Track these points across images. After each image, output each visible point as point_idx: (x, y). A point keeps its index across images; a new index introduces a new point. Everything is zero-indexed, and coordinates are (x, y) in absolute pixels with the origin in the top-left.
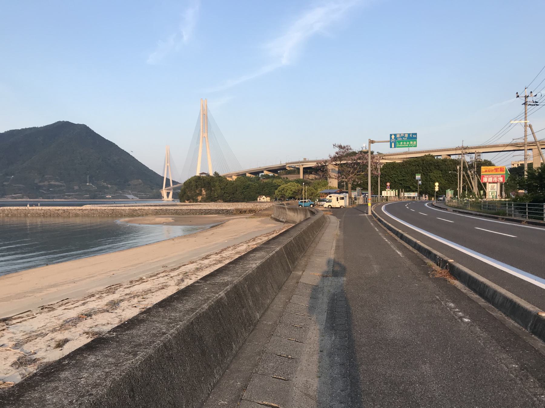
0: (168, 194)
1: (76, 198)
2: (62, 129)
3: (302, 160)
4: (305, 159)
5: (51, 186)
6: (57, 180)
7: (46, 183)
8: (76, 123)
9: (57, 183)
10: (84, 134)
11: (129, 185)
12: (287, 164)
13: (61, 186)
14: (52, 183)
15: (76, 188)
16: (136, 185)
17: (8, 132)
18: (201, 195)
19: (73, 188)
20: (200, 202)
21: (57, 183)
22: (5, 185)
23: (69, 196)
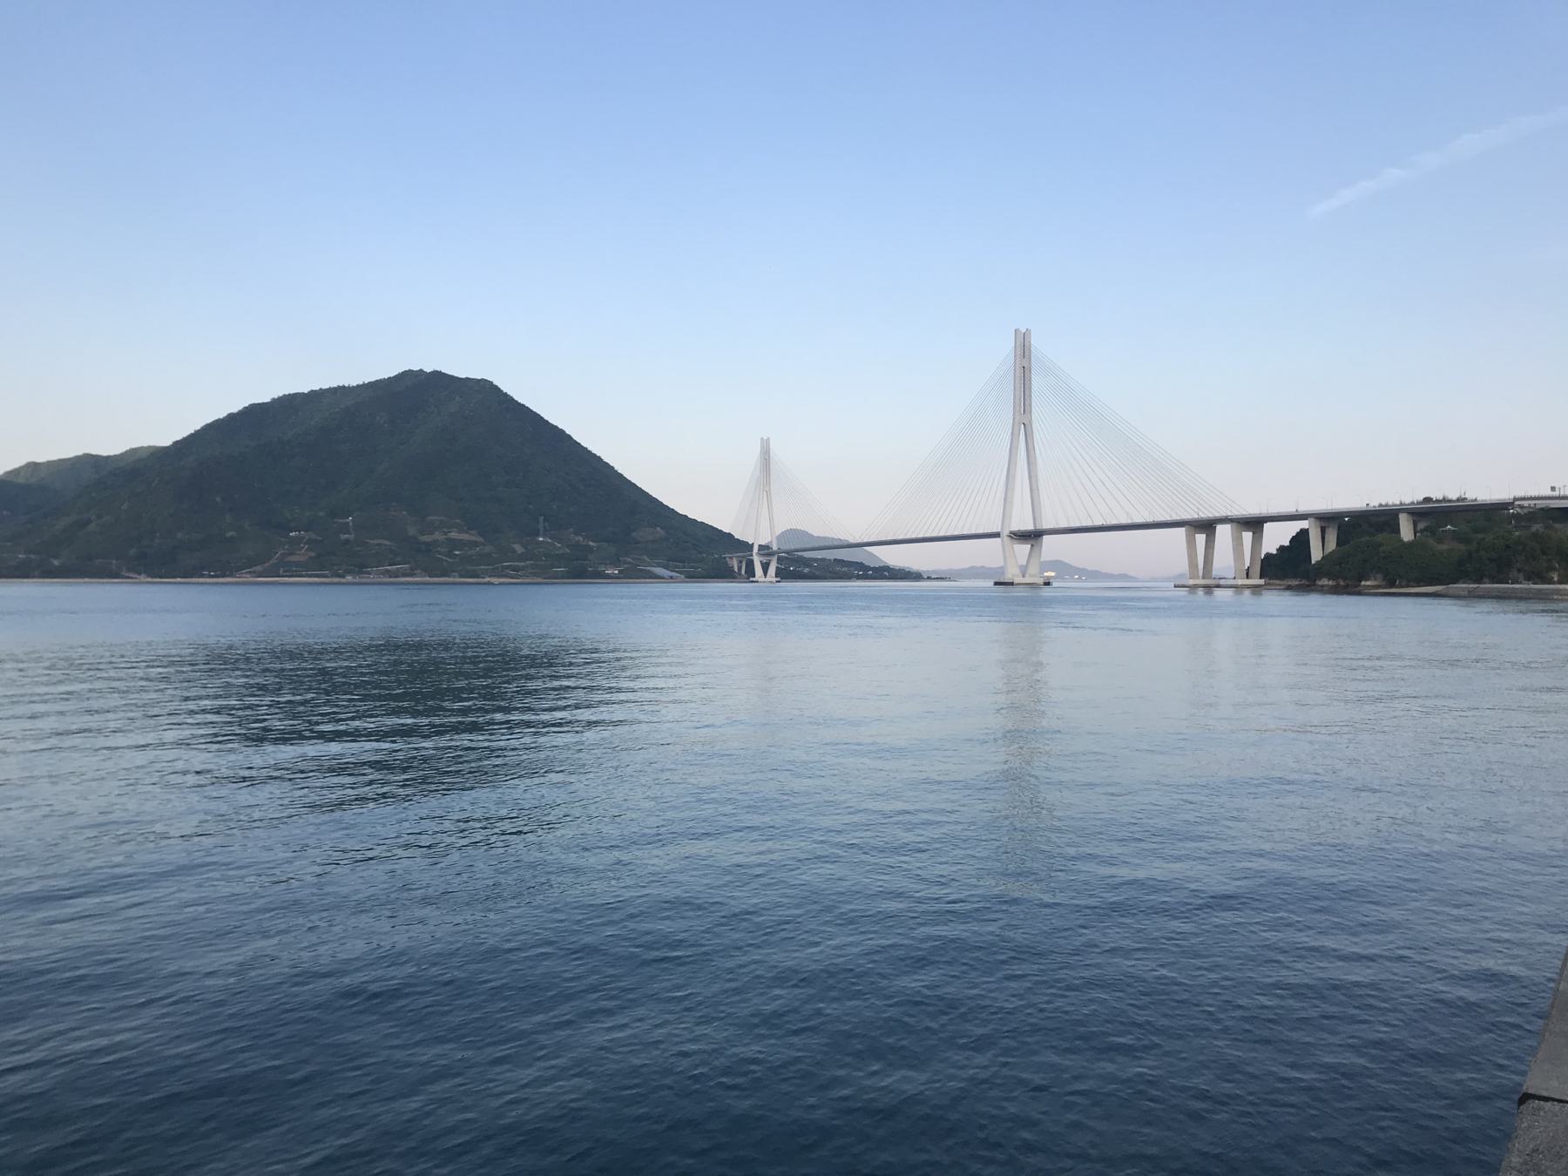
0: (765, 567)
1: (535, 575)
2: (419, 393)
3: (1549, 493)
4: (1553, 489)
7: (438, 536)
8: (463, 376)
9: (465, 537)
12: (1516, 499)
13: (476, 544)
14: (454, 535)
15: (519, 549)
18: (1554, 569)
19: (514, 551)
20: (1560, 582)
21: (465, 537)
22: (347, 541)
23: (516, 569)
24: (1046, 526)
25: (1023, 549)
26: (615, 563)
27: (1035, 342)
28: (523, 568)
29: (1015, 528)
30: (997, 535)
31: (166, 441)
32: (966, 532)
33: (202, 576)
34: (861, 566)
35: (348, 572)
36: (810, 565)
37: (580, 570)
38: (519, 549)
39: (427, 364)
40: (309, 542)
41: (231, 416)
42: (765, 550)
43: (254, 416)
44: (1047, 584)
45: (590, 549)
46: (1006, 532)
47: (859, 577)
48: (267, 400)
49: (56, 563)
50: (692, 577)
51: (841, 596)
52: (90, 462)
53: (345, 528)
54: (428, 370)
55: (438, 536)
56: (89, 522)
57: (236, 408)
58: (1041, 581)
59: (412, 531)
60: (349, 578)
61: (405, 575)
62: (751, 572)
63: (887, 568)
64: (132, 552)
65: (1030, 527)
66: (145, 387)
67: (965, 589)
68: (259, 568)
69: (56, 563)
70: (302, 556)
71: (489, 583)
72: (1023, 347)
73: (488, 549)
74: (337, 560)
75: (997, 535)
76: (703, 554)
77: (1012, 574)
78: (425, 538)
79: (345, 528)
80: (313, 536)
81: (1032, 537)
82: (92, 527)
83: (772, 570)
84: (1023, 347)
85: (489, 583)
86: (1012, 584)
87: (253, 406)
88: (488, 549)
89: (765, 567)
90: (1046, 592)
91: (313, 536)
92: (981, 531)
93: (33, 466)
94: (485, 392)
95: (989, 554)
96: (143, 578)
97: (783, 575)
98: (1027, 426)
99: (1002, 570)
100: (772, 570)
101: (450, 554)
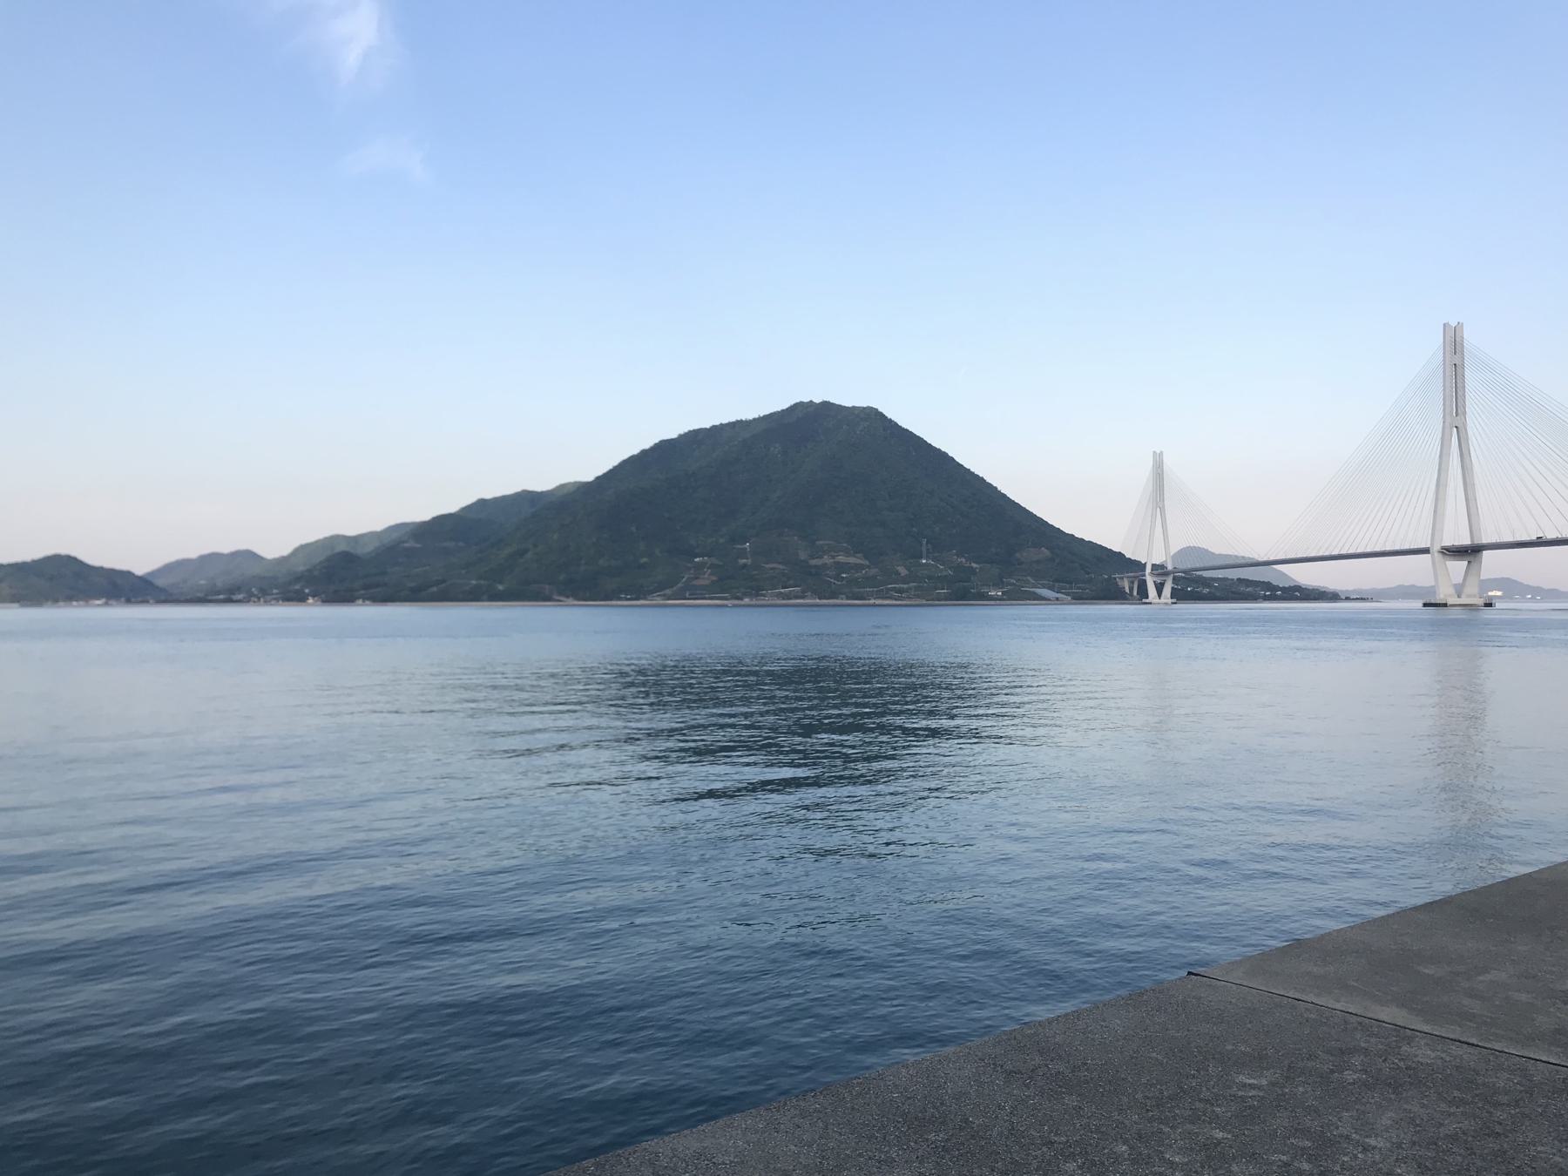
0: (1160, 588)
1: (918, 597)
5: (841, 567)
6: (848, 554)
7: (827, 560)
9: (852, 560)
10: (872, 428)
11: (1021, 563)
13: (861, 567)
14: (841, 558)
15: (903, 571)
16: (1038, 562)
17: (686, 435)
19: (898, 573)
21: (852, 560)
22: (745, 566)
23: (900, 591)
24: (1485, 540)
25: (1458, 566)
26: (998, 584)
27: (1470, 338)
28: (907, 591)
29: (1448, 543)
30: (1426, 551)
31: (589, 476)
32: (1388, 548)
33: (620, 599)
34: (1268, 586)
35: (745, 595)
36: (1205, 585)
37: (963, 592)
38: (903, 571)
39: (816, 394)
40: (712, 566)
41: (644, 453)
42: (1159, 569)
43: (664, 450)
44: (1489, 605)
45: (973, 571)
46: (1437, 548)
47: (1266, 598)
48: (674, 436)
49: (501, 587)
50: (1079, 598)
51: (1240, 621)
52: (527, 499)
53: (743, 554)
54: (817, 400)
55: (827, 560)
56: (526, 551)
57: (647, 445)
58: (1481, 602)
59: (803, 556)
60: (746, 600)
61: (797, 597)
62: (1143, 593)
63: (1298, 588)
64: (562, 577)
65: (1466, 541)
66: (571, 429)
67: (1390, 611)
68: (668, 592)
69: (501, 587)
70: (706, 579)
71: (874, 605)
72: (1454, 343)
73: (874, 571)
74: (736, 584)
75: (1426, 551)
76: (1091, 575)
77: (1445, 593)
78: (813, 562)
79: (743, 554)
80: (714, 561)
81: (1470, 552)
82: (529, 555)
83: (1167, 591)
84: (1454, 343)
85: (874, 605)
86: (1445, 605)
87: (662, 442)
88: (874, 571)
89: (1160, 588)
90: (1488, 614)
91: (714, 561)
92: (1406, 547)
93: (482, 503)
94: (872, 419)
95: (1417, 571)
96: (571, 601)
97: (1179, 595)
98: (1461, 431)
99: (1432, 590)
100: (1167, 591)
101: (838, 577)
